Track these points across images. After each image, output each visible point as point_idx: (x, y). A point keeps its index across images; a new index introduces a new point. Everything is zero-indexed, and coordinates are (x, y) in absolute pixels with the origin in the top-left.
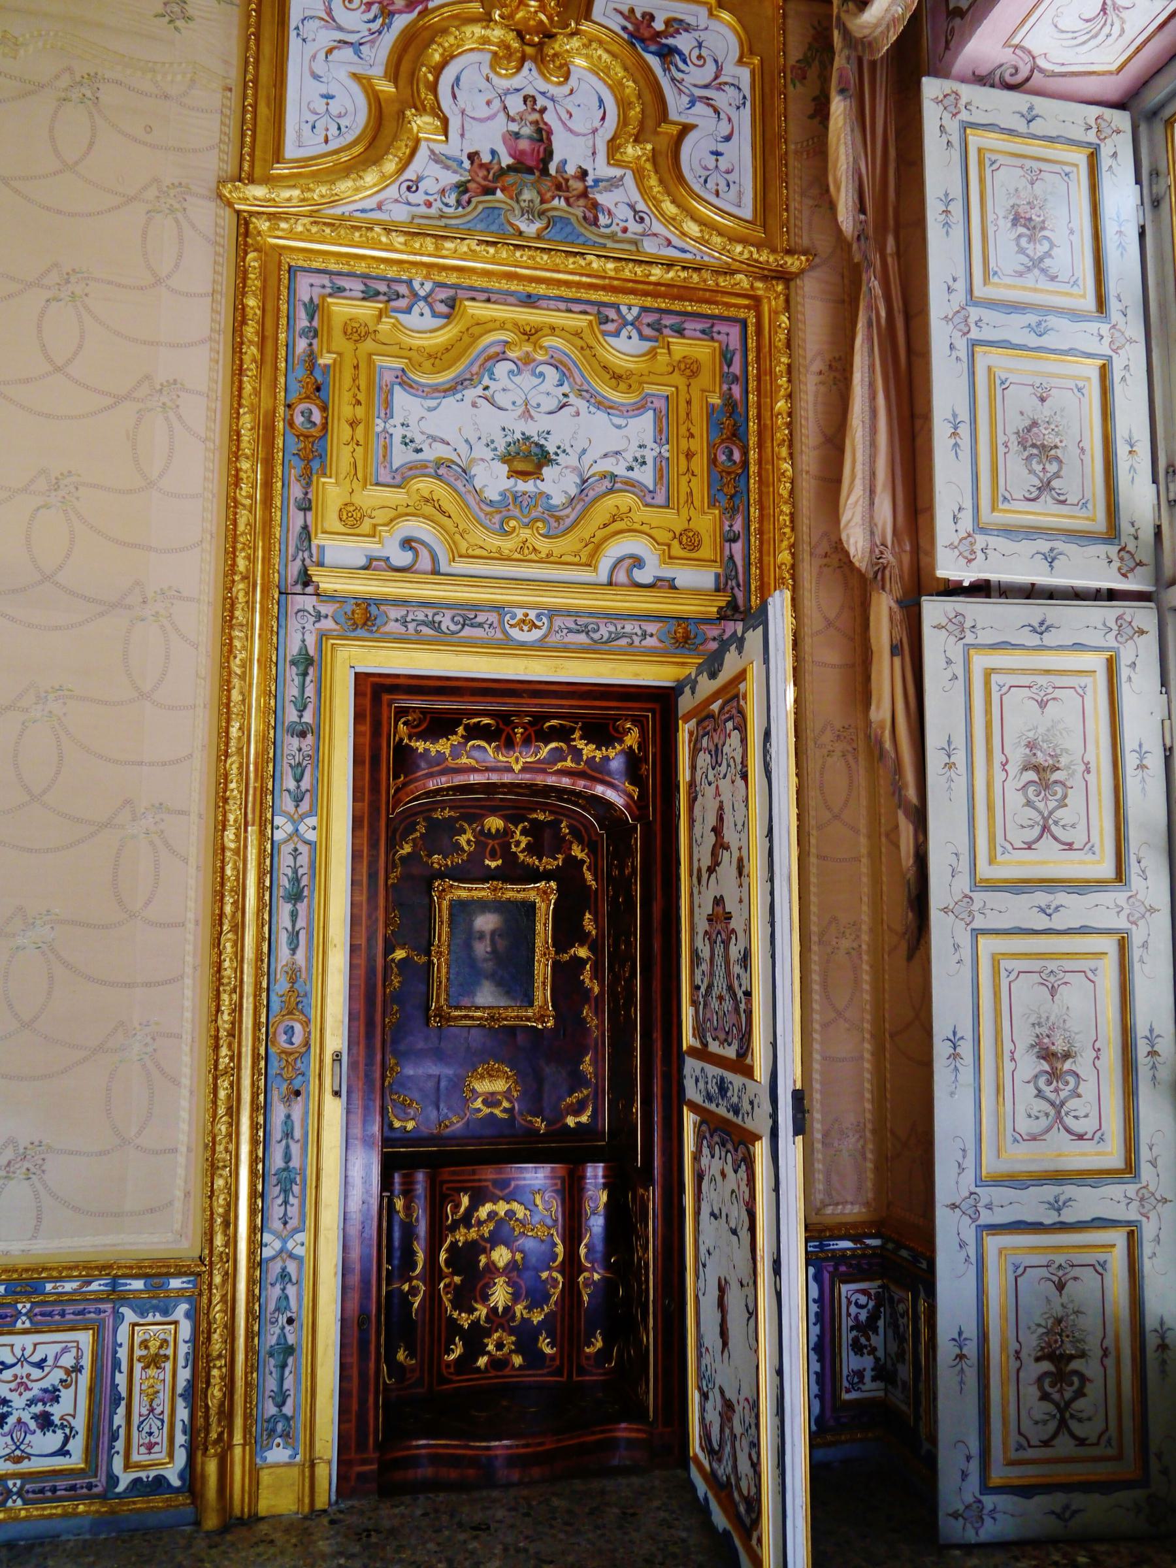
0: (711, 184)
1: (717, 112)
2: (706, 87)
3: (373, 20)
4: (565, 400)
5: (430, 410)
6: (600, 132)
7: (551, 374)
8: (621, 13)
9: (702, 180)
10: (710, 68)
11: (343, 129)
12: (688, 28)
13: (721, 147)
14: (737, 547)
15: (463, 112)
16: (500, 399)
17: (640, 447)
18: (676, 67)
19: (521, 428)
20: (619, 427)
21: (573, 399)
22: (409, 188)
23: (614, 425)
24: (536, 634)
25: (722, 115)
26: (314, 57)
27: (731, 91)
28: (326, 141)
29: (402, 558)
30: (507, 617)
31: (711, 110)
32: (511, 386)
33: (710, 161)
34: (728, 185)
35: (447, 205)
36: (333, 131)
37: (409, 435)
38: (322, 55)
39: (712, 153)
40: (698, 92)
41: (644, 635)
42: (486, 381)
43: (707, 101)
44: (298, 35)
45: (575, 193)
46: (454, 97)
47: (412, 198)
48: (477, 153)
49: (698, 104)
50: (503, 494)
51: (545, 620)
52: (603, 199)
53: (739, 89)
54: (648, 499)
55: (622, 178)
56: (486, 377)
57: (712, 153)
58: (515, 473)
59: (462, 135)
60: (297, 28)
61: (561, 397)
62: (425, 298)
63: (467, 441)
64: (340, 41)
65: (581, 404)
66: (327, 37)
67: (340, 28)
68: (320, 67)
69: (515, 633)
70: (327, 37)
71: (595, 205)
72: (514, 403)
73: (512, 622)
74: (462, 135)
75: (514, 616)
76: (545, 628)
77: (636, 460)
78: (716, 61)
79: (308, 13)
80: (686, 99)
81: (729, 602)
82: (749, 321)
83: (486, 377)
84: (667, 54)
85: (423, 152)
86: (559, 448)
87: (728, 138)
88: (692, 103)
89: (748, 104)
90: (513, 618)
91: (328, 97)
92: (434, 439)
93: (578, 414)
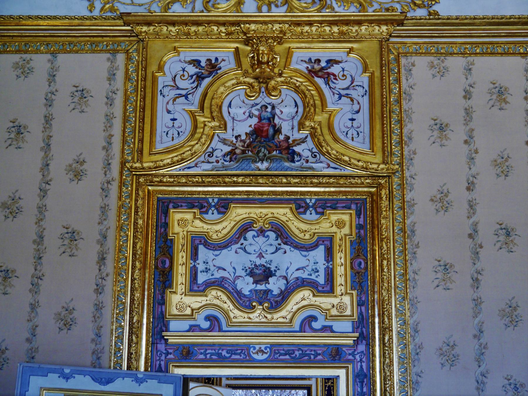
0: (350, 135)
1: (352, 100)
2: (347, 88)
3: (194, 82)
4: (279, 246)
5: (216, 256)
6: (296, 118)
7: (272, 235)
8: (305, 61)
9: (345, 133)
10: (349, 79)
11: (181, 134)
12: (337, 62)
13: (354, 117)
14: (363, 308)
15: (233, 118)
16: (248, 249)
17: (315, 263)
18: (332, 81)
19: (258, 262)
20: (305, 256)
21: (283, 246)
22: (209, 156)
23: (302, 255)
24: (265, 356)
25: (355, 101)
26: (168, 103)
27: (360, 89)
28: (173, 140)
29: (206, 325)
30: (252, 349)
31: (349, 99)
32: (253, 242)
33: (349, 124)
34: (358, 134)
35: (225, 161)
36: (176, 135)
37: (208, 267)
38: (171, 102)
39: (350, 120)
40: (343, 92)
41: (317, 355)
42: (242, 241)
43: (347, 95)
44: (161, 94)
45: (284, 147)
46: (229, 113)
47: (211, 160)
48: (240, 136)
49: (343, 98)
50: (250, 291)
51: (268, 349)
52: (297, 149)
53: (363, 87)
54: (320, 289)
55: (306, 137)
56: (242, 239)
57: (350, 120)
58: (256, 282)
59: (233, 130)
60: (161, 91)
61: (277, 245)
62: (214, 206)
63: (234, 268)
64: (179, 94)
65: (287, 248)
66: (174, 93)
67: (178, 88)
68: (170, 107)
69: (255, 356)
70: (174, 93)
71: (294, 152)
72: (255, 251)
73: (254, 351)
74: (233, 130)
75: (255, 348)
76: (268, 354)
77: (313, 270)
78: (351, 76)
79: (166, 84)
80: (337, 96)
81: (358, 338)
82: (368, 200)
83: (242, 239)
84: (328, 77)
85: (216, 138)
86: (276, 267)
87: (358, 112)
88: (340, 98)
89: (367, 94)
91: (174, 120)
92: (220, 268)
93: (285, 252)
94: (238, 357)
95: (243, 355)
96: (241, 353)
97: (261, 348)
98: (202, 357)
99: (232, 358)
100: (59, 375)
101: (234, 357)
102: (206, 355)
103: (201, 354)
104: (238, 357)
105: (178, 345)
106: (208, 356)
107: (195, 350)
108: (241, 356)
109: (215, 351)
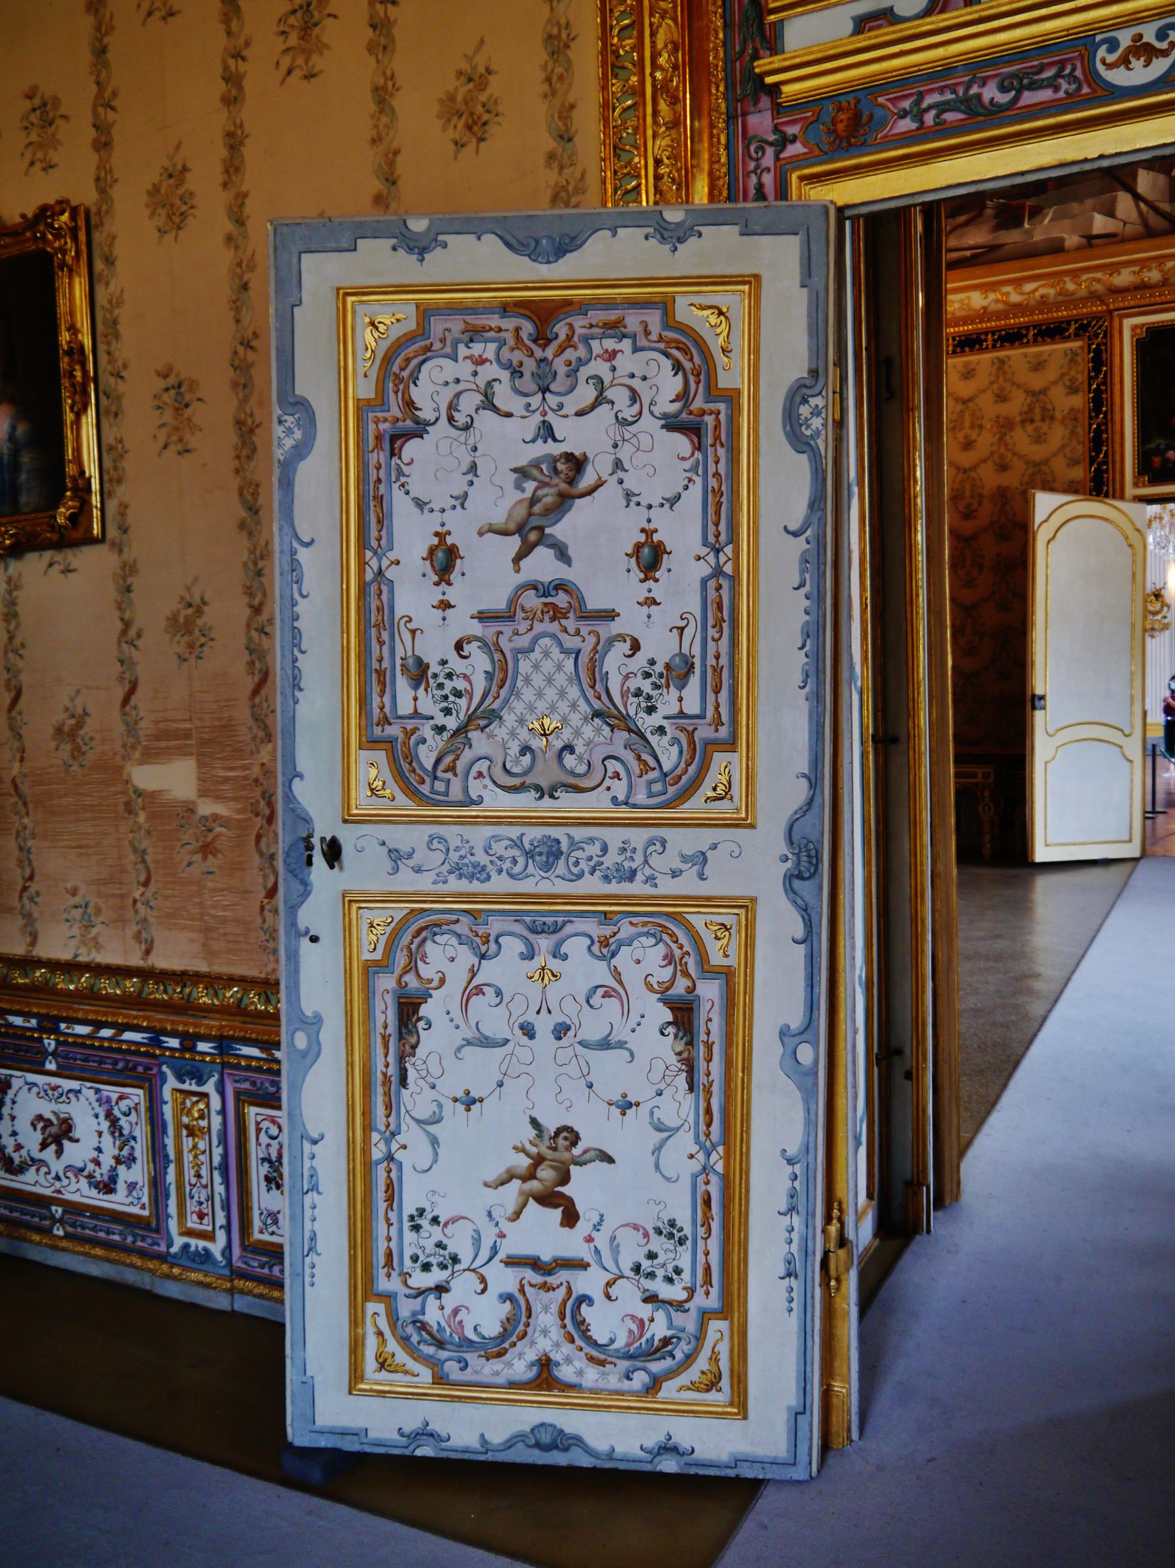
30: (1102, 52)
69: (1119, 77)
73: (1111, 58)
75: (1113, 45)
90: (1111, 50)
94: (1046, 95)
95: (1064, 86)
96: (1058, 75)
97: (1141, 36)
98: (907, 125)
99: (1021, 103)
100: (394, 241)
101: (1028, 98)
102: (919, 116)
103: (904, 114)
104: (1046, 95)
105: (814, 102)
106: (929, 118)
107: (882, 106)
108: (1057, 89)
109: (954, 92)
